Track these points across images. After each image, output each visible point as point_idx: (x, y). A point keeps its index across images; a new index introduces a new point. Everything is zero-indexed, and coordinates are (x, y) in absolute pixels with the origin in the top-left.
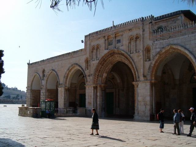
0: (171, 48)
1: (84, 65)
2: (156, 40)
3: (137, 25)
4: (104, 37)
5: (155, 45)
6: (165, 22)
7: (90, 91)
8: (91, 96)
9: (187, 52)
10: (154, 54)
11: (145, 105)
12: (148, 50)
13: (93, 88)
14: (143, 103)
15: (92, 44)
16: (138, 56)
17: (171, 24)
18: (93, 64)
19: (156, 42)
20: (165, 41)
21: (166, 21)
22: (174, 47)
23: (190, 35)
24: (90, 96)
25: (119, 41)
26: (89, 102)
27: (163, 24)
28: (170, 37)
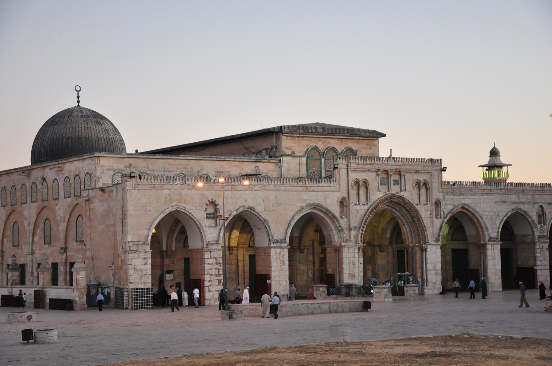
0: (463, 208)
1: (336, 210)
2: (447, 194)
3: (426, 168)
4: (378, 170)
5: (446, 199)
6: (356, 143)
7: (352, 255)
8: (354, 264)
9: (477, 215)
10: (446, 211)
11: (437, 274)
12: (438, 204)
13: (357, 250)
14: (433, 272)
15: (354, 176)
16: (427, 210)
17: (364, 148)
18: (357, 211)
19: (447, 197)
20: (456, 197)
21: (357, 141)
22: (466, 207)
23: (481, 197)
24: (351, 264)
25: (396, 182)
26: (349, 274)
27: (353, 145)
28: (461, 193)
